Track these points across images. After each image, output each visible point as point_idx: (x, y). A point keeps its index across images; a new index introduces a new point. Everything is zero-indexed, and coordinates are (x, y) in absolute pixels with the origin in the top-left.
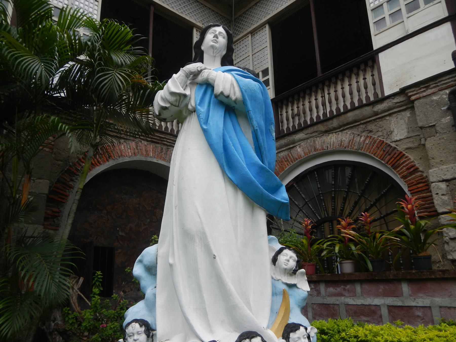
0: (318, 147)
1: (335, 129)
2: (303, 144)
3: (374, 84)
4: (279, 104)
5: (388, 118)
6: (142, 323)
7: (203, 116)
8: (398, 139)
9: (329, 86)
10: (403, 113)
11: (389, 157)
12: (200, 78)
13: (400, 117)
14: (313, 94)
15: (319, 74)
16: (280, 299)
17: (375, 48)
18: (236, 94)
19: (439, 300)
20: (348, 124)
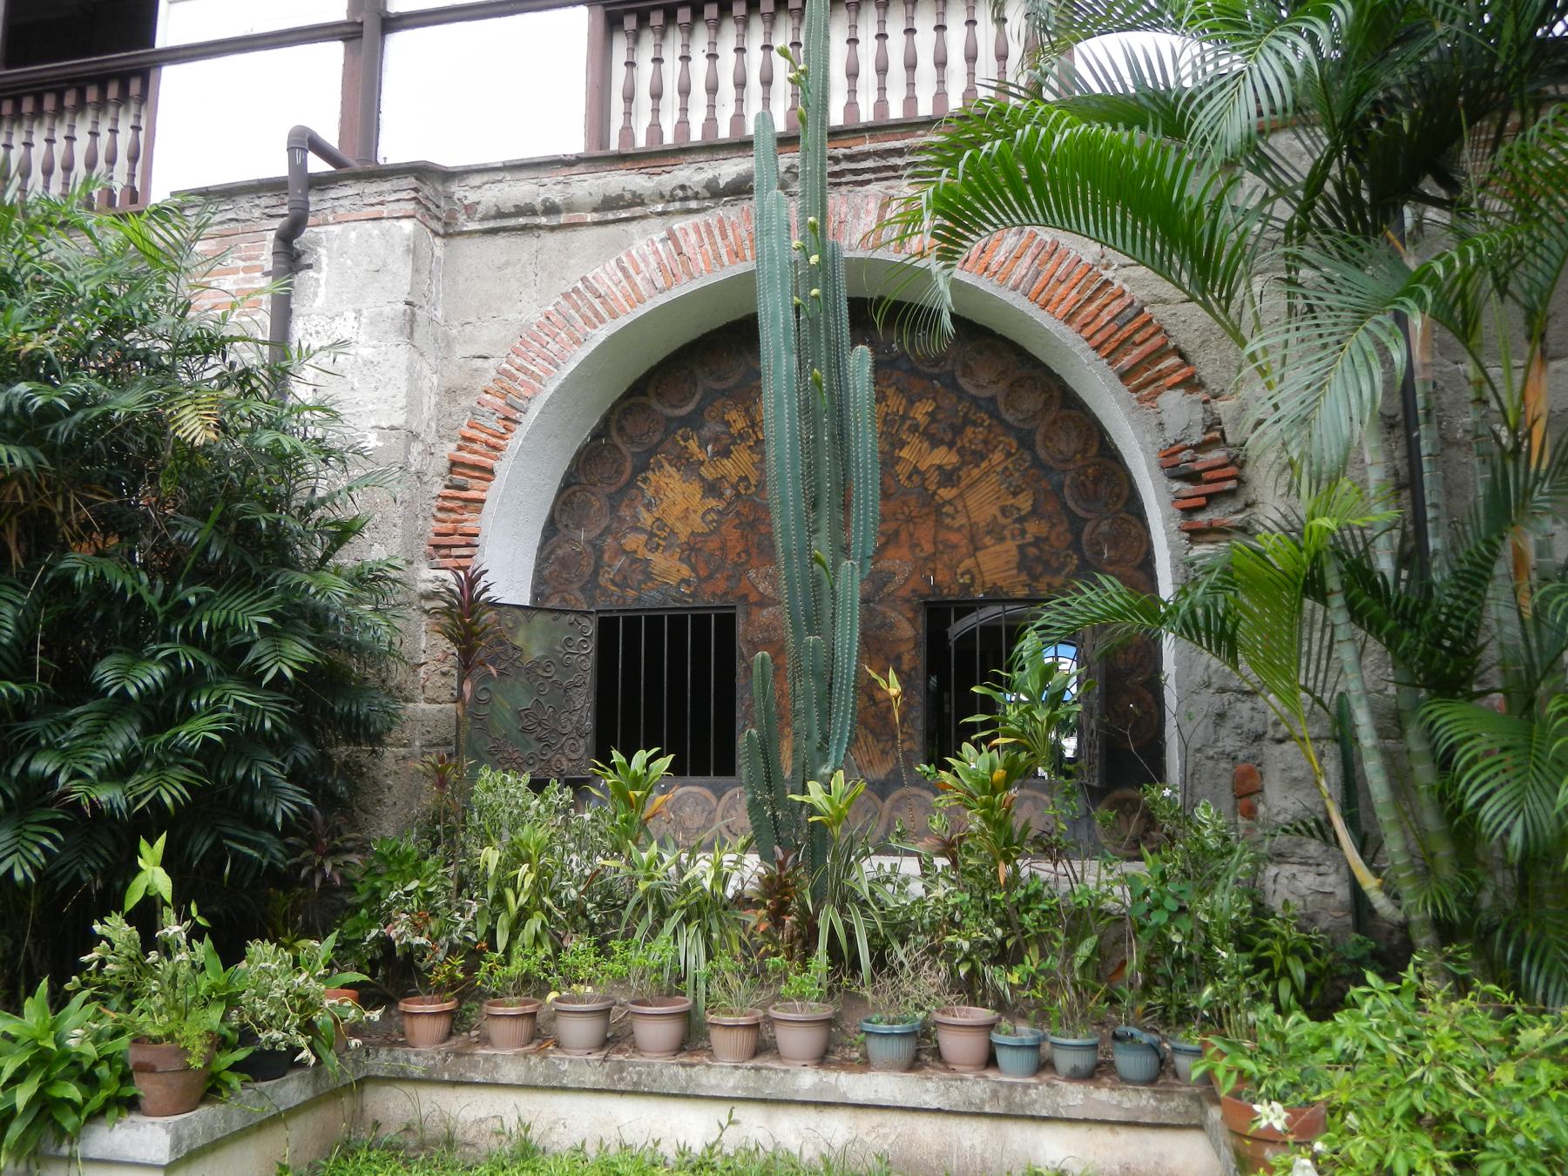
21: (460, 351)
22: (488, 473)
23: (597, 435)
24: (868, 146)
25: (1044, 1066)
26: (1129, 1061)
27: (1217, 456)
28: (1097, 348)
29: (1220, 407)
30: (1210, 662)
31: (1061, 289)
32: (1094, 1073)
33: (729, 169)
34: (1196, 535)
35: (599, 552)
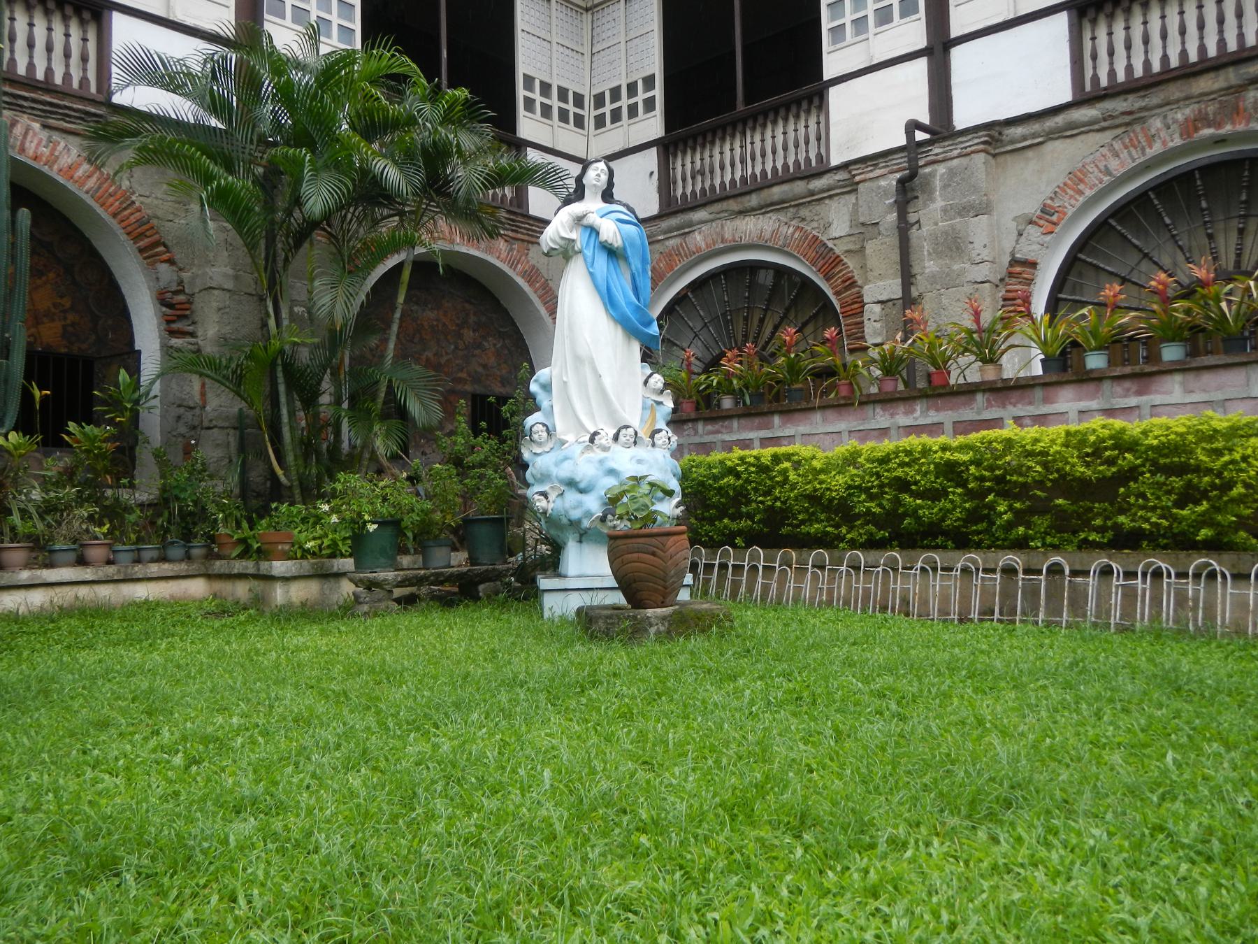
0: (728, 236)
1: (753, 209)
2: (705, 228)
3: (819, 139)
4: (671, 149)
5: (827, 201)
7: (589, 260)
8: (837, 235)
9: (753, 129)
10: (847, 197)
11: (822, 262)
12: (585, 222)
13: (842, 201)
14: (728, 138)
15: (740, 106)
16: (648, 412)
17: (825, 78)
18: (617, 243)
19: (803, 429)
20: (772, 204)
25: (138, 561)
26: (176, 552)
27: (181, 298)
28: (128, 234)
29: (186, 275)
31: (111, 199)
32: (163, 559)
34: (173, 333)
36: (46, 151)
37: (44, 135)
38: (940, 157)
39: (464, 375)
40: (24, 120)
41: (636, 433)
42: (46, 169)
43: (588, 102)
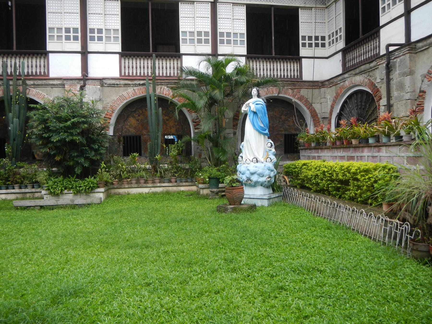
0: (353, 82)
1: (358, 73)
5: (376, 70)
6: (241, 156)
18: (255, 111)
20: (362, 72)
21: (105, 102)
22: (110, 119)
23: (121, 113)
24: (159, 81)
26: (189, 180)
27: (198, 120)
30: (196, 143)
32: (186, 182)
33: (142, 82)
34: (196, 129)
35: (122, 128)
36: (168, 93)
37: (168, 88)
38: (397, 56)
39: (282, 129)
40: (163, 87)
41: (257, 160)
42: (168, 97)
43: (327, 38)
